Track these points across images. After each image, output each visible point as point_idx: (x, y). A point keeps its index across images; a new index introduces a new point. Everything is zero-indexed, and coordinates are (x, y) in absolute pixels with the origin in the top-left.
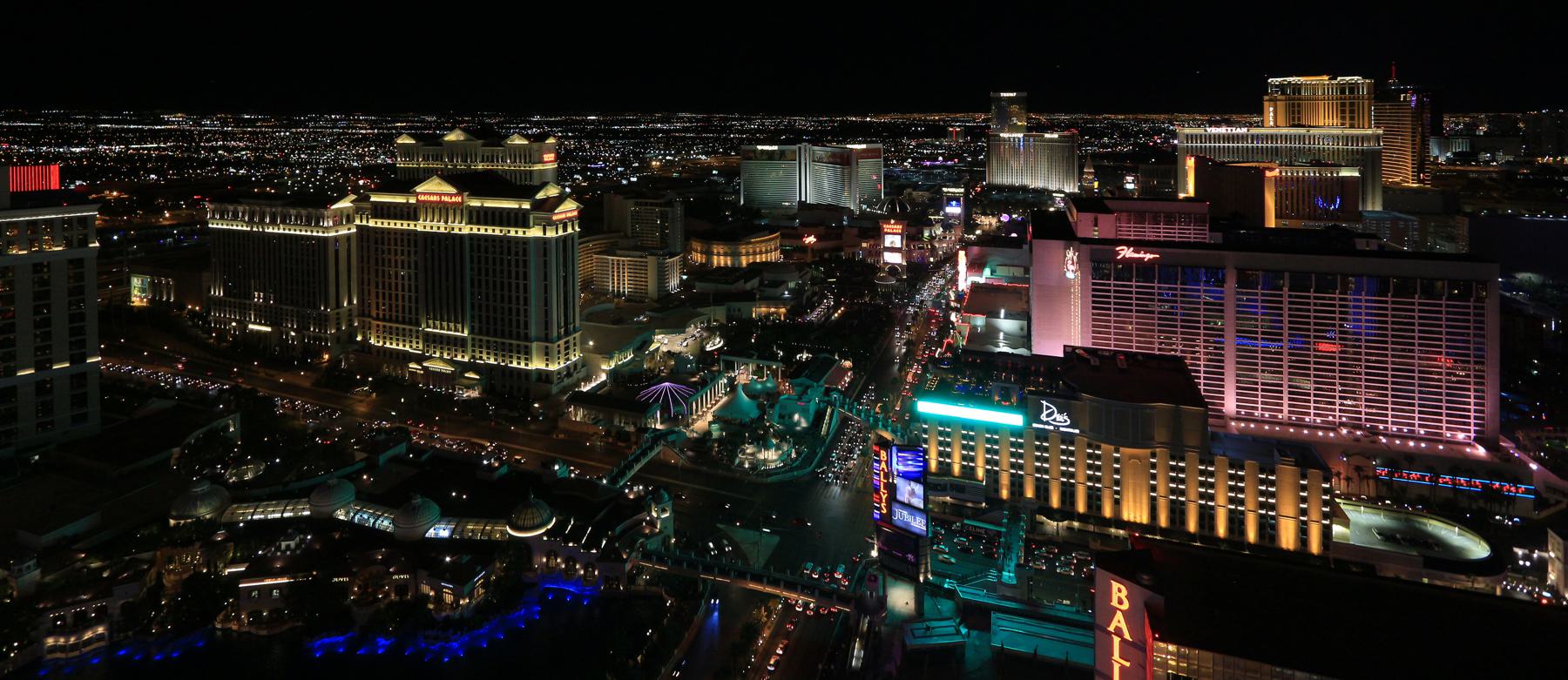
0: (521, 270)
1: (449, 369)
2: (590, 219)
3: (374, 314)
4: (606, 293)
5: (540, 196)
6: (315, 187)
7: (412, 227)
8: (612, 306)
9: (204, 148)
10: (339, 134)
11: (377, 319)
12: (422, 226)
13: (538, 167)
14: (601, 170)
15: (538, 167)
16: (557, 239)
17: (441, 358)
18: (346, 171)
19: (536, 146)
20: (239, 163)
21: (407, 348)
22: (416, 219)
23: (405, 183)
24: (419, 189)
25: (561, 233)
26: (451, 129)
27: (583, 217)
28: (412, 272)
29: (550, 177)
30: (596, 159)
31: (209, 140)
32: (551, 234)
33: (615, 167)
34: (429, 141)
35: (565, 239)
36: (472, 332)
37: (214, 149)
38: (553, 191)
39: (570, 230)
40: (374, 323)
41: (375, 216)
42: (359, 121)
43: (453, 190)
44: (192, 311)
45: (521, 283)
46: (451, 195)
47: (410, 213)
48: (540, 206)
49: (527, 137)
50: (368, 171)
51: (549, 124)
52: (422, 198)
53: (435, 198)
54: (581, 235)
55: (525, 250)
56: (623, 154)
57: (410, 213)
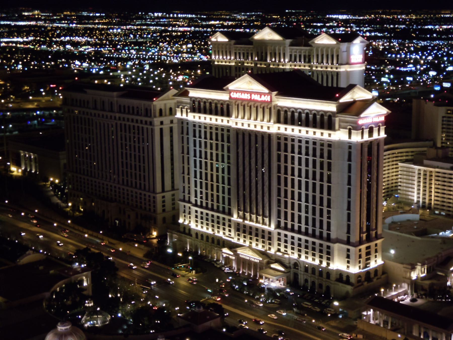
0: (326, 172)
1: (256, 258)
2: (400, 126)
3: (193, 200)
4: (409, 203)
5: (347, 98)
6: (142, 80)
7: (225, 123)
8: (416, 217)
9: (56, 43)
10: (161, 32)
11: (196, 205)
12: (237, 122)
13: (343, 69)
14: (411, 73)
15: (343, 69)
16: (362, 144)
17: (250, 247)
18: (168, 67)
19: (344, 46)
20: (82, 57)
21: (221, 234)
22: (229, 115)
23: (220, 79)
24: (231, 86)
25: (366, 137)
26: (261, 27)
27: (389, 122)
28: (226, 165)
29: (357, 79)
30: (405, 63)
31: (59, 36)
32: (356, 138)
33: (426, 71)
34: (241, 39)
35: (370, 144)
36: (278, 226)
37: (63, 44)
38: (360, 94)
39: (375, 136)
40: (194, 208)
41: (194, 110)
42: (177, 19)
43: (266, 91)
44: (53, 183)
45: (326, 185)
46: (261, 94)
47: (223, 110)
48: (345, 109)
49: (335, 36)
50: (185, 66)
51: (358, 23)
52: (234, 95)
53: (246, 96)
54: (387, 141)
55: (329, 152)
56: (436, 57)
57: (223, 110)
